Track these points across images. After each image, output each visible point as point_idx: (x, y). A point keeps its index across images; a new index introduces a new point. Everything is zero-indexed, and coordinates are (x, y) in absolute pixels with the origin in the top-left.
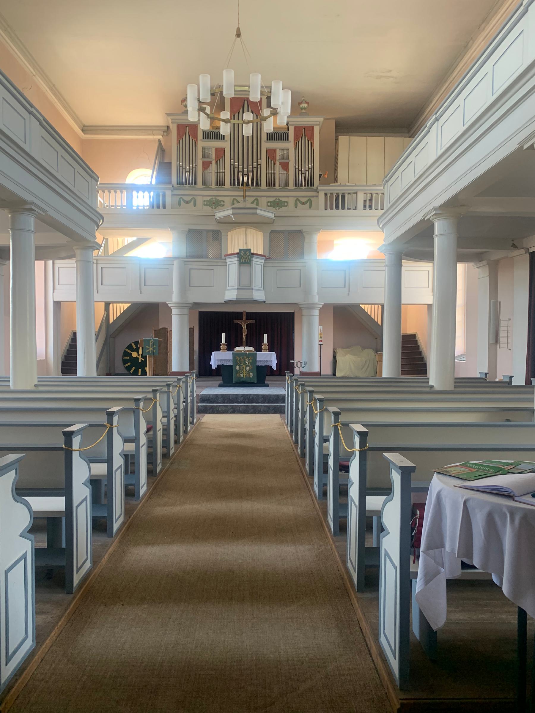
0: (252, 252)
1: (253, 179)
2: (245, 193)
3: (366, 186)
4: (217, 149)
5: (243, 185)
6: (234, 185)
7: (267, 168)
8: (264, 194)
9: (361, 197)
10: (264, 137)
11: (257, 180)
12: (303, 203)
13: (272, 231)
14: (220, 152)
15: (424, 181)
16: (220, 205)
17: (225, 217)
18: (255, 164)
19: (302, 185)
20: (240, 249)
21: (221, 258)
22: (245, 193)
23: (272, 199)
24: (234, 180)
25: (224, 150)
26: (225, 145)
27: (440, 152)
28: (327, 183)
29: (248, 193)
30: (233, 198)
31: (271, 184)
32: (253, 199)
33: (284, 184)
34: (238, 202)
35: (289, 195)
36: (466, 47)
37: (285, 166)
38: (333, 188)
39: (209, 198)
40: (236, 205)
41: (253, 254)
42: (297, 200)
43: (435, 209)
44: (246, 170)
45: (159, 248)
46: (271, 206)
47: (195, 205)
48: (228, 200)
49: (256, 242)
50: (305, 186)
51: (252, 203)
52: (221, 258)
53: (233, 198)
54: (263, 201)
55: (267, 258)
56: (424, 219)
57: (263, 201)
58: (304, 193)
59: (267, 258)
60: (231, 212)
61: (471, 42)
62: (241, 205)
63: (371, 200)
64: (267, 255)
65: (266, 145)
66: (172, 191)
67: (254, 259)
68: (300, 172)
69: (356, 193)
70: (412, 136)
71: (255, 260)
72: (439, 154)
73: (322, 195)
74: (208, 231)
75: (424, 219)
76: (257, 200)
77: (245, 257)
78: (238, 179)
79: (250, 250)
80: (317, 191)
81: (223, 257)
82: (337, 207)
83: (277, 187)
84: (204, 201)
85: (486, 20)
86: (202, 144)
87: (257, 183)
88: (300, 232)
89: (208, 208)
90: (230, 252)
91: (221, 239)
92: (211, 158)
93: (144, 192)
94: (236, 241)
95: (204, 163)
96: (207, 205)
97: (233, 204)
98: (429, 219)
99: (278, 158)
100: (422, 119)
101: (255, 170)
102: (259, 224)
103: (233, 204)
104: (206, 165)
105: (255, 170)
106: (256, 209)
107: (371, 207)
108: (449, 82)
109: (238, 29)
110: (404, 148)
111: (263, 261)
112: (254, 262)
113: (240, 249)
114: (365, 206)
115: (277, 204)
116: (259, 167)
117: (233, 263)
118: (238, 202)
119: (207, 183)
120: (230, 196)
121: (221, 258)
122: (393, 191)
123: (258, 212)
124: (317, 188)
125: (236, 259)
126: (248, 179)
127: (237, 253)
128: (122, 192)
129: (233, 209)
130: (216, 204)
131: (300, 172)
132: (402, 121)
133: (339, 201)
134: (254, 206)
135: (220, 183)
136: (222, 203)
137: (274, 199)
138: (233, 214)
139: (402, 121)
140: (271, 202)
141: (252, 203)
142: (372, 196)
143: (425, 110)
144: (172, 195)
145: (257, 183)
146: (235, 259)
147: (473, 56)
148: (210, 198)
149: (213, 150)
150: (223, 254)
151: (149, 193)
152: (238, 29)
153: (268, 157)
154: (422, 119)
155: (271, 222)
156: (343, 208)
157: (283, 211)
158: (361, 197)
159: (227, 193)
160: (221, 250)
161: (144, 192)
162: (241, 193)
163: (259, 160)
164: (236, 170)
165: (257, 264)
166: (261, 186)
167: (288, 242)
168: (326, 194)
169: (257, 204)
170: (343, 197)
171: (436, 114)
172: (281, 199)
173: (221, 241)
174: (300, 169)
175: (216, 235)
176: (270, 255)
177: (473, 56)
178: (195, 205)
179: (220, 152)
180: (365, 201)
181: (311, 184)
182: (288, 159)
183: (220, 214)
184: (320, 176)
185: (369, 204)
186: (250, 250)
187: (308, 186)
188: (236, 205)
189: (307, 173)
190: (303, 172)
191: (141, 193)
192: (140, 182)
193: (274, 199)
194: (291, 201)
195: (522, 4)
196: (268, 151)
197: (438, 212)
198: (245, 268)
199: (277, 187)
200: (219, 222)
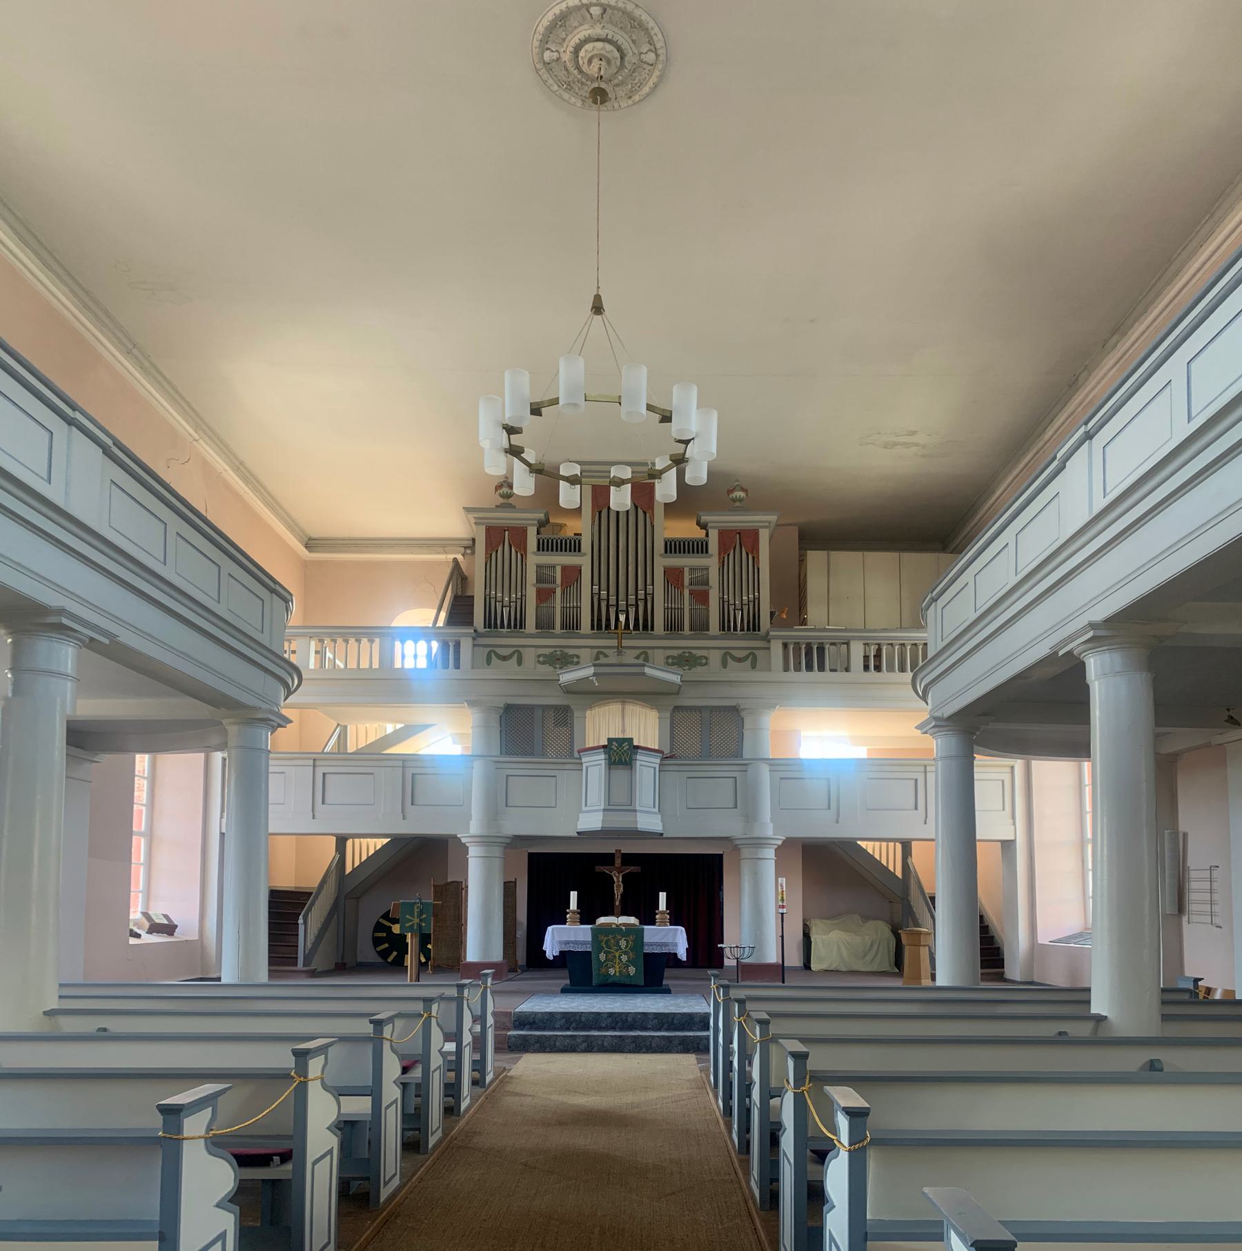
0: (635, 743)
1: (637, 619)
2: (620, 643)
3: (865, 630)
4: (565, 568)
5: (616, 627)
6: (600, 627)
7: (666, 600)
8: (659, 644)
9: (857, 651)
10: (659, 547)
11: (645, 620)
12: (740, 660)
13: (677, 709)
14: (572, 575)
15: (1054, 571)
16: (572, 663)
17: (580, 680)
18: (641, 593)
19: (735, 629)
20: (609, 739)
21: (572, 754)
22: (620, 643)
23: (675, 653)
24: (599, 620)
25: (578, 570)
26: (583, 561)
27: (1100, 503)
28: (786, 625)
29: (625, 643)
30: (595, 651)
31: (673, 626)
32: (638, 652)
33: (700, 627)
34: (606, 656)
35: (711, 646)
36: (1073, 385)
37: (701, 597)
38: (797, 633)
39: (547, 651)
40: (603, 660)
41: (638, 747)
42: (726, 654)
43: (1092, 626)
44: (622, 603)
45: (446, 738)
46: (673, 664)
47: (520, 662)
48: (585, 655)
49: (645, 726)
50: (742, 630)
51: (637, 658)
52: (572, 756)
53: (595, 651)
54: (659, 656)
55: (667, 758)
56: (1056, 653)
57: (659, 656)
58: (739, 644)
59: (667, 758)
60: (591, 671)
61: (1085, 373)
62: (613, 659)
63: (878, 656)
64: (667, 751)
65: (662, 562)
66: (474, 639)
67: (638, 757)
68: (732, 608)
69: (848, 644)
70: (959, 550)
71: (641, 758)
72: (1096, 510)
73: (777, 648)
74: (545, 708)
75: (1056, 653)
76: (646, 653)
77: (621, 754)
78: (608, 619)
79: (631, 739)
80: (767, 638)
81: (576, 755)
82: (809, 668)
83: (687, 631)
84: (539, 656)
85: (1119, 328)
86: (534, 559)
87: (645, 625)
88: (735, 710)
89: (547, 668)
90: (590, 744)
91: (572, 724)
92: (554, 582)
93: (416, 642)
94: (602, 724)
95: (539, 592)
96: (544, 663)
97: (597, 658)
98: (1069, 653)
99: (686, 582)
100: (986, 508)
101: (641, 604)
102: (651, 695)
103: (597, 658)
104: (544, 595)
105: (641, 604)
106: (644, 665)
107: (878, 668)
108: (1035, 451)
109: (598, 298)
110: (939, 574)
111: (658, 761)
112: (638, 763)
113: (609, 739)
114: (866, 668)
115: (685, 661)
116: (649, 598)
117: (595, 766)
118: (606, 656)
119: (544, 624)
120: (592, 647)
121: (572, 756)
122: (933, 636)
123: (648, 670)
124: (768, 634)
125: (603, 756)
126: (627, 619)
127: (604, 747)
128: (371, 641)
129: (594, 665)
130: (563, 660)
131: (732, 608)
132: (935, 526)
133: (812, 657)
134: (640, 661)
135: (571, 625)
136: (575, 660)
137: (680, 652)
138: (595, 674)
139: (935, 526)
140: (673, 657)
141: (637, 658)
142: (879, 651)
143: (975, 513)
144: (474, 645)
145: (645, 625)
146: (601, 757)
147: (1091, 396)
148: (551, 650)
149: (558, 569)
150: (576, 749)
151: (428, 642)
152: (598, 298)
153: (667, 581)
154: (986, 508)
155: (676, 691)
156: (821, 668)
157: (698, 673)
158: (857, 651)
159: (585, 643)
160: (572, 742)
161: (416, 642)
162: (614, 643)
163: (649, 587)
164: (604, 604)
165: (646, 769)
166: (652, 629)
167: (712, 735)
168: (785, 646)
169: (646, 660)
170: (821, 650)
171: (1086, 423)
172: (694, 652)
173: (572, 727)
174: (732, 602)
175: (563, 716)
176: (672, 748)
177: (1091, 396)
178: (520, 662)
179: (572, 575)
180: (866, 658)
181: (754, 625)
182: (707, 584)
183: (568, 676)
184: (772, 614)
185: (874, 662)
186: (631, 739)
187: (748, 629)
188: (603, 660)
189: (745, 608)
190: (738, 607)
191: (409, 644)
192: (414, 633)
193: (680, 652)
194: (715, 657)
195: (1055, 458)
196: (667, 571)
197: (1100, 633)
198: (620, 774)
199: (687, 631)
200: (568, 690)
